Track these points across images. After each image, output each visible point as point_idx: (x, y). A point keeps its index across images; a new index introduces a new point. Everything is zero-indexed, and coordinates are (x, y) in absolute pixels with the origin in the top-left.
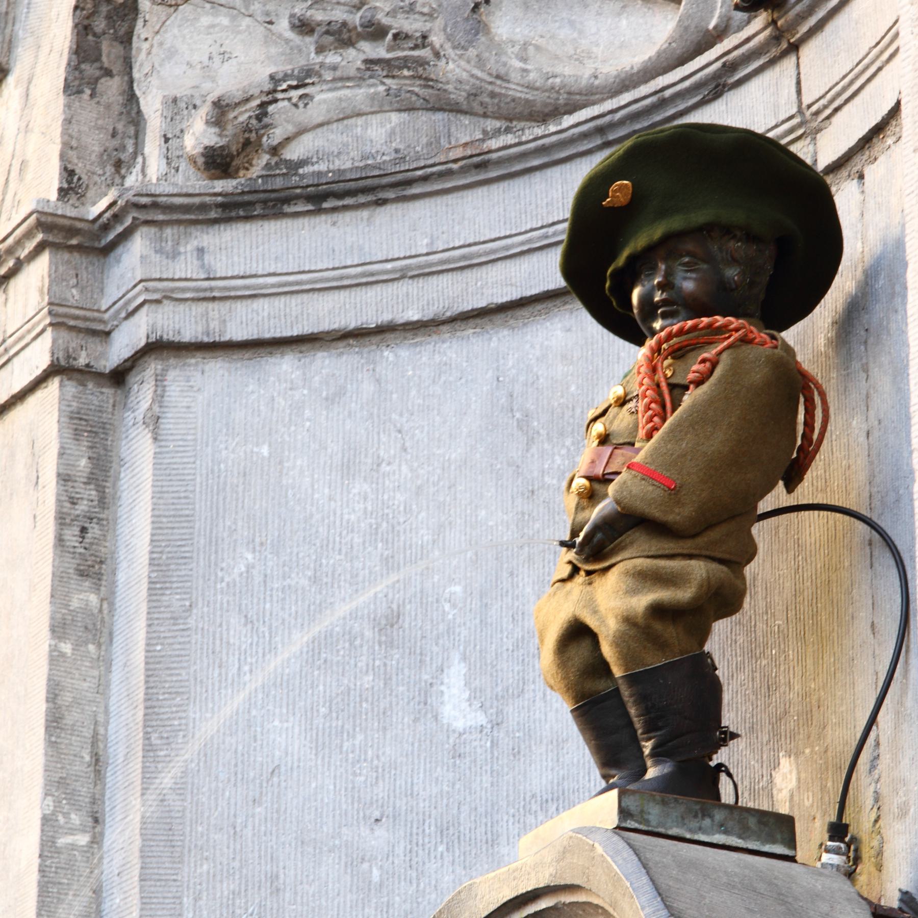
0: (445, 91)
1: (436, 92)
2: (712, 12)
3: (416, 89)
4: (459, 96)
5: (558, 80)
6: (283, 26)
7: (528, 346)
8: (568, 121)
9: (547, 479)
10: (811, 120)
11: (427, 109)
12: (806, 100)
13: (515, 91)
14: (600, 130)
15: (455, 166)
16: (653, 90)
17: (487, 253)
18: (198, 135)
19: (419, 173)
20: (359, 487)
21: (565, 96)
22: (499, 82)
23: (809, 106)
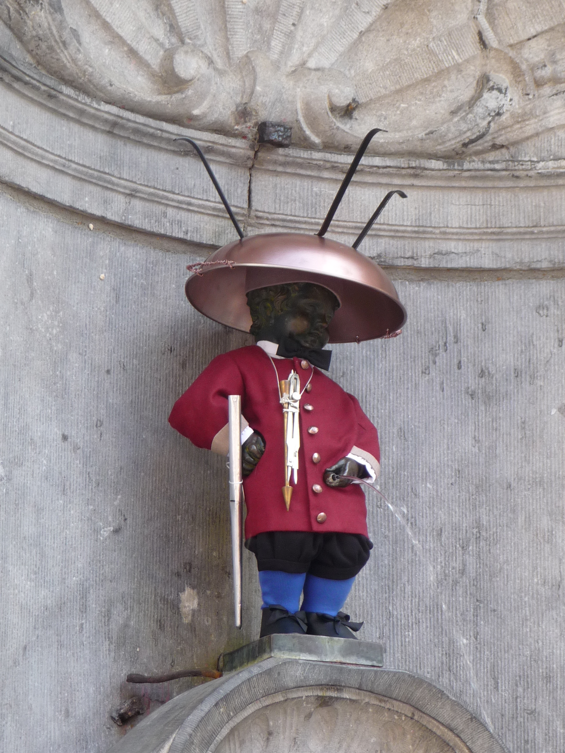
0: (25, 22)
1: (19, 19)
3: (11, 9)
4: (29, 31)
5: (90, 70)
7: (34, 228)
9: (39, 326)
10: (253, 219)
11: (6, 24)
12: (255, 205)
13: (64, 57)
14: (115, 124)
15: (43, 88)
16: (157, 127)
17: (33, 153)
19: (28, 78)
21: (86, 80)
22: (61, 45)
23: (257, 211)
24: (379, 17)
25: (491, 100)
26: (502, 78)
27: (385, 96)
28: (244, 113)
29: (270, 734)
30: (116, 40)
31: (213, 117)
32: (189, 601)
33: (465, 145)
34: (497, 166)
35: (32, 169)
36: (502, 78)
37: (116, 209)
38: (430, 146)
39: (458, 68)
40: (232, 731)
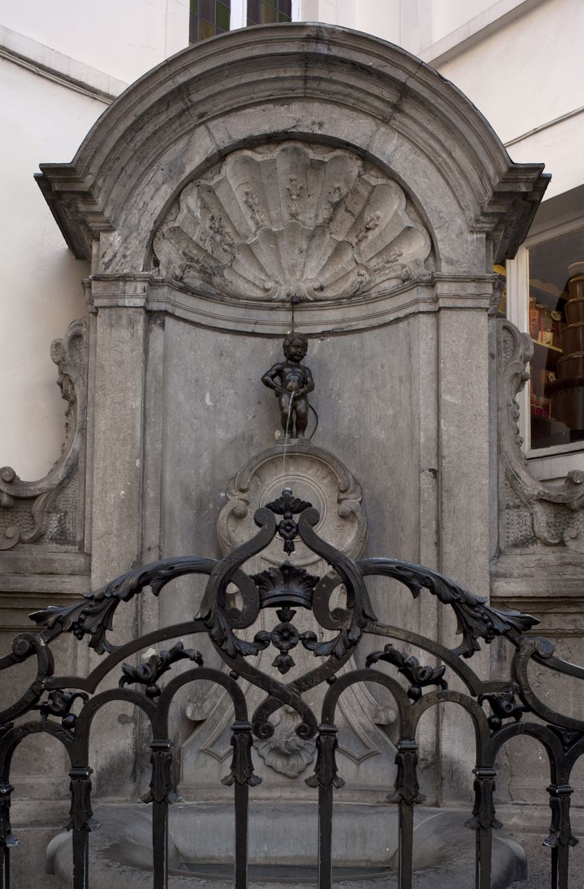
2: (274, 295)
6: (181, 252)
8: (241, 301)
14: (246, 305)
18: (178, 272)
20: (192, 352)
24: (327, 261)
26: (363, 272)
27: (333, 283)
28: (288, 295)
29: (277, 466)
30: (248, 282)
31: (280, 298)
32: (278, 434)
33: (354, 293)
35: (219, 321)
36: (363, 272)
37: (250, 329)
38: (344, 295)
39: (352, 271)
40: (261, 467)
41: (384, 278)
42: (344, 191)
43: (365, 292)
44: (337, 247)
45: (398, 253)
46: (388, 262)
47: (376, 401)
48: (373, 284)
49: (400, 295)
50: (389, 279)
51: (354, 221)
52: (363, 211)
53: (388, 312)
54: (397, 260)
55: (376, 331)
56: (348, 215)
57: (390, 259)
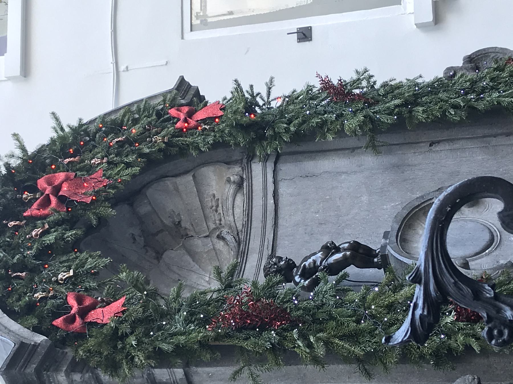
24: (197, 264)
25: (224, 234)
33: (236, 242)
34: (243, 231)
39: (213, 245)
41: (231, 211)
42: (137, 232)
43: (238, 234)
44: (186, 251)
45: (212, 197)
46: (216, 211)
47: (350, 217)
48: (233, 224)
49: (253, 188)
50: (233, 207)
51: (167, 233)
52: (162, 221)
53: (265, 206)
54: (218, 199)
55: (280, 222)
56: (160, 235)
57: (214, 208)
